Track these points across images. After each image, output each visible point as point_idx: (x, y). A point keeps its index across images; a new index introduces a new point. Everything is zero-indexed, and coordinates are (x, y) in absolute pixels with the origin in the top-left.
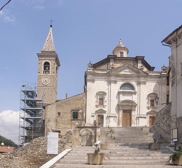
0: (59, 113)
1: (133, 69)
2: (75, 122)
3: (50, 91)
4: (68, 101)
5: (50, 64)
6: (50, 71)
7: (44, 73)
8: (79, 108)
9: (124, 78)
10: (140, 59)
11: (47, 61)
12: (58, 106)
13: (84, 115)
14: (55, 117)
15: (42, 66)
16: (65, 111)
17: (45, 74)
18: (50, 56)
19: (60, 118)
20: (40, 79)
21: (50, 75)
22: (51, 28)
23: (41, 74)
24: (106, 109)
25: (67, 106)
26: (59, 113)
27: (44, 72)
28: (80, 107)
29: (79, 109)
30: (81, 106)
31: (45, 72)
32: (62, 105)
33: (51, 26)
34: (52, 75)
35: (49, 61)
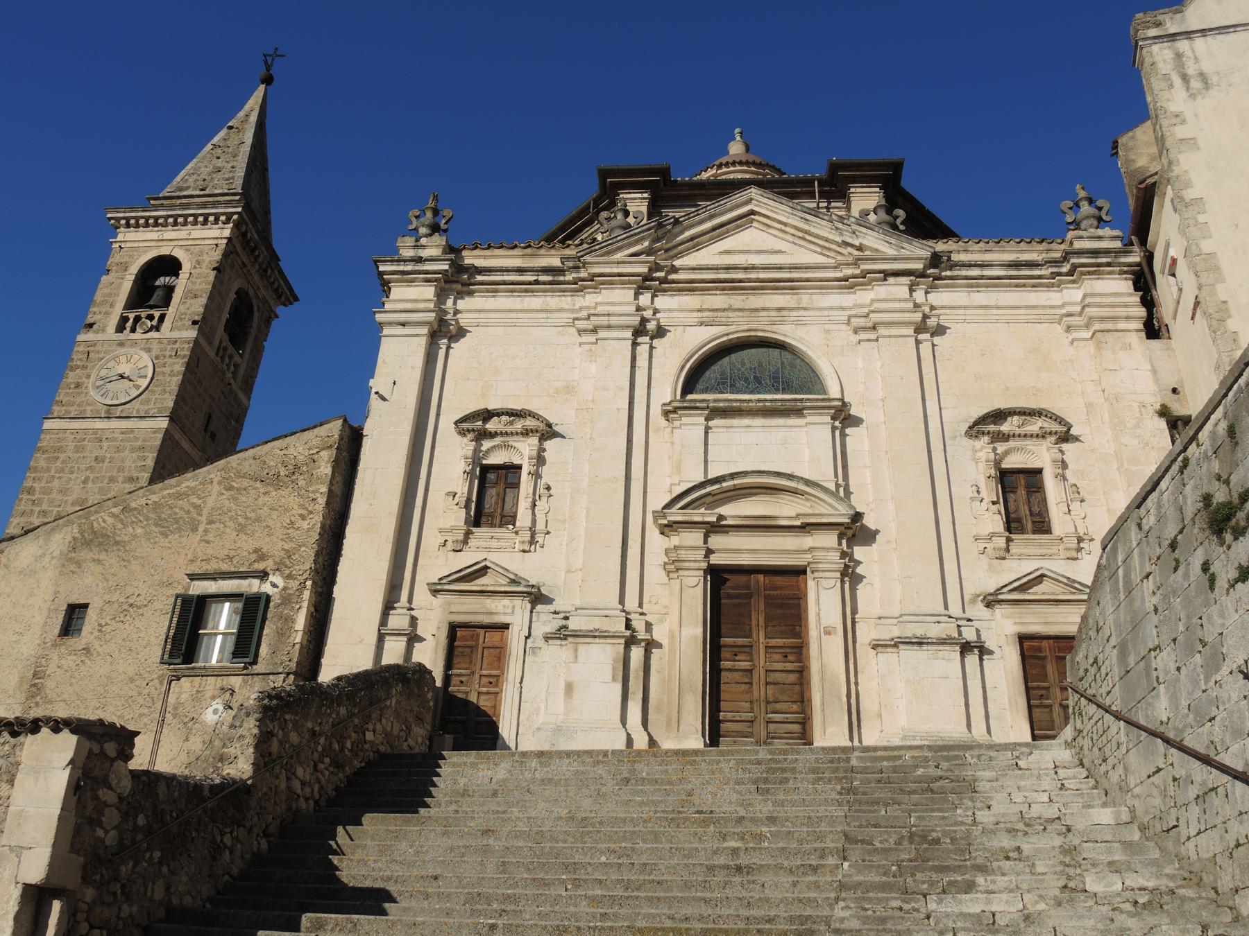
0: (74, 616)
1: (805, 227)
2: (197, 697)
3: (133, 450)
4: (179, 496)
5: (186, 267)
6: (171, 311)
7: (120, 328)
8: (262, 557)
9: (718, 300)
10: (868, 180)
11: (165, 251)
12: (87, 544)
13: (300, 622)
14: (28, 647)
15: (120, 285)
16: (129, 590)
17: (133, 330)
18: (195, 216)
19: (69, 661)
20: (85, 367)
21: (160, 341)
22: (262, 87)
23: (100, 337)
24: (531, 568)
25: (162, 541)
26: (74, 616)
27: (124, 320)
28: (275, 547)
29: (260, 566)
30: (289, 538)
31: (129, 324)
32: (124, 535)
33: (268, 80)
34: (176, 334)
35: (179, 254)
